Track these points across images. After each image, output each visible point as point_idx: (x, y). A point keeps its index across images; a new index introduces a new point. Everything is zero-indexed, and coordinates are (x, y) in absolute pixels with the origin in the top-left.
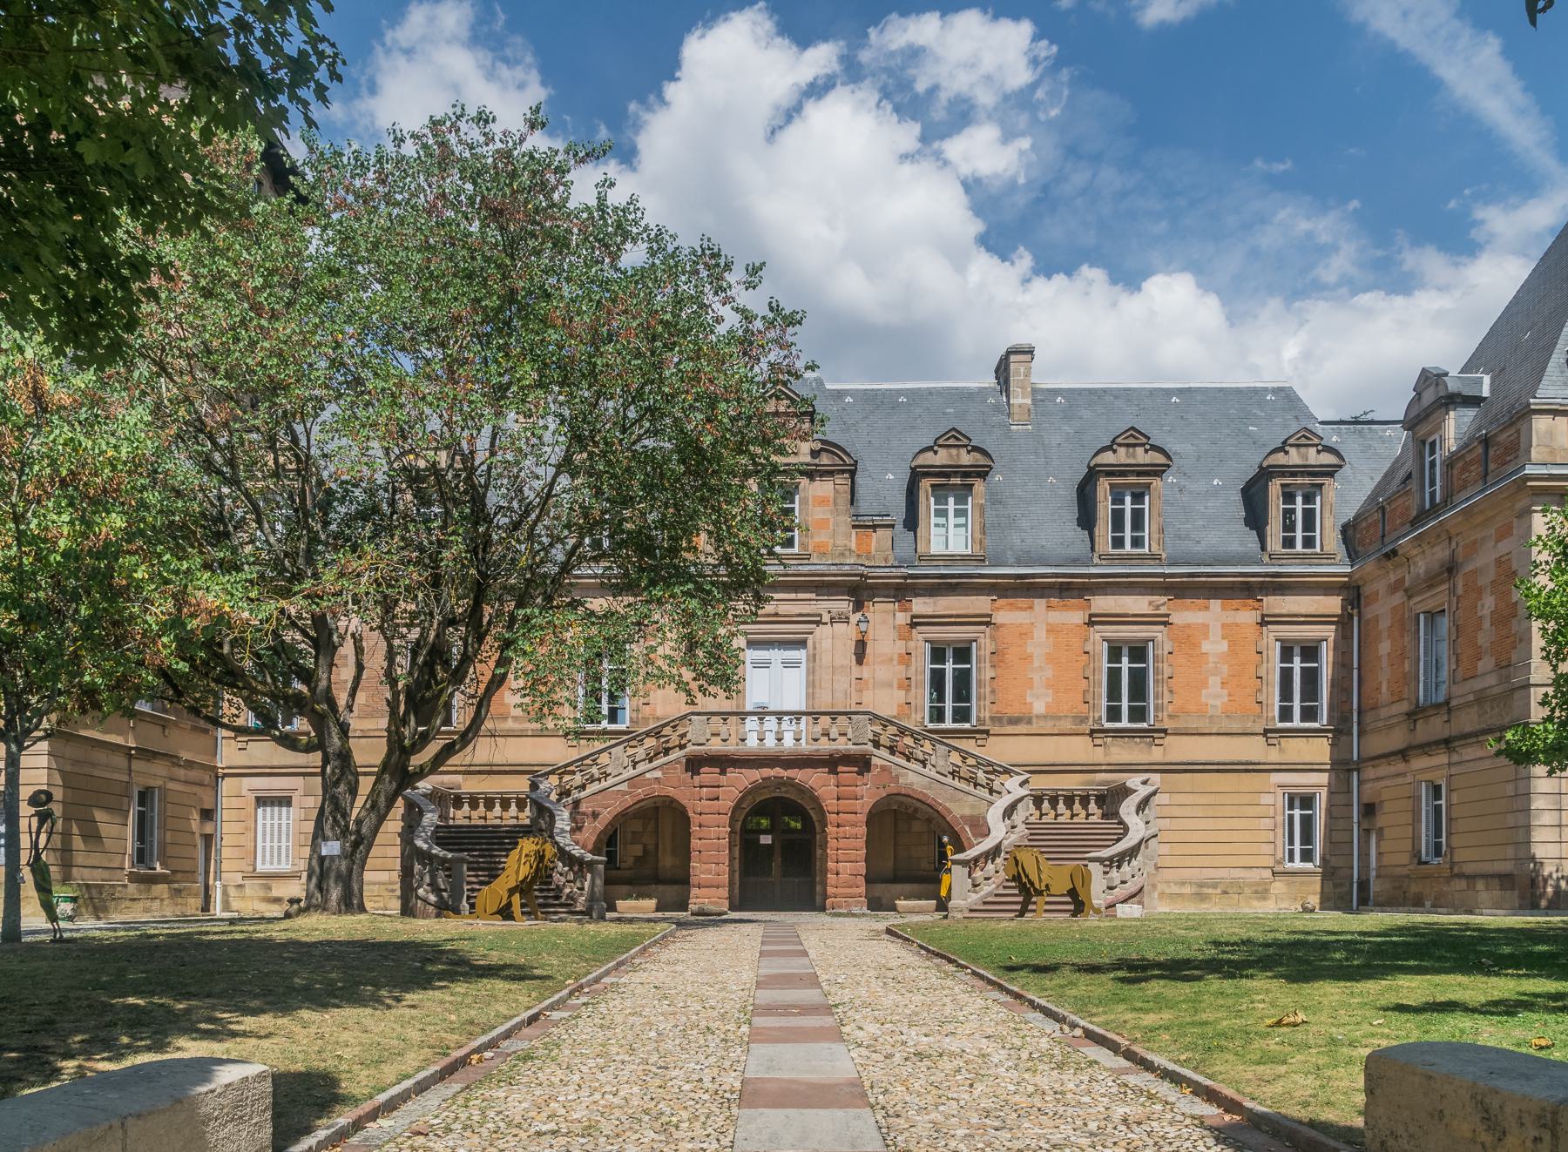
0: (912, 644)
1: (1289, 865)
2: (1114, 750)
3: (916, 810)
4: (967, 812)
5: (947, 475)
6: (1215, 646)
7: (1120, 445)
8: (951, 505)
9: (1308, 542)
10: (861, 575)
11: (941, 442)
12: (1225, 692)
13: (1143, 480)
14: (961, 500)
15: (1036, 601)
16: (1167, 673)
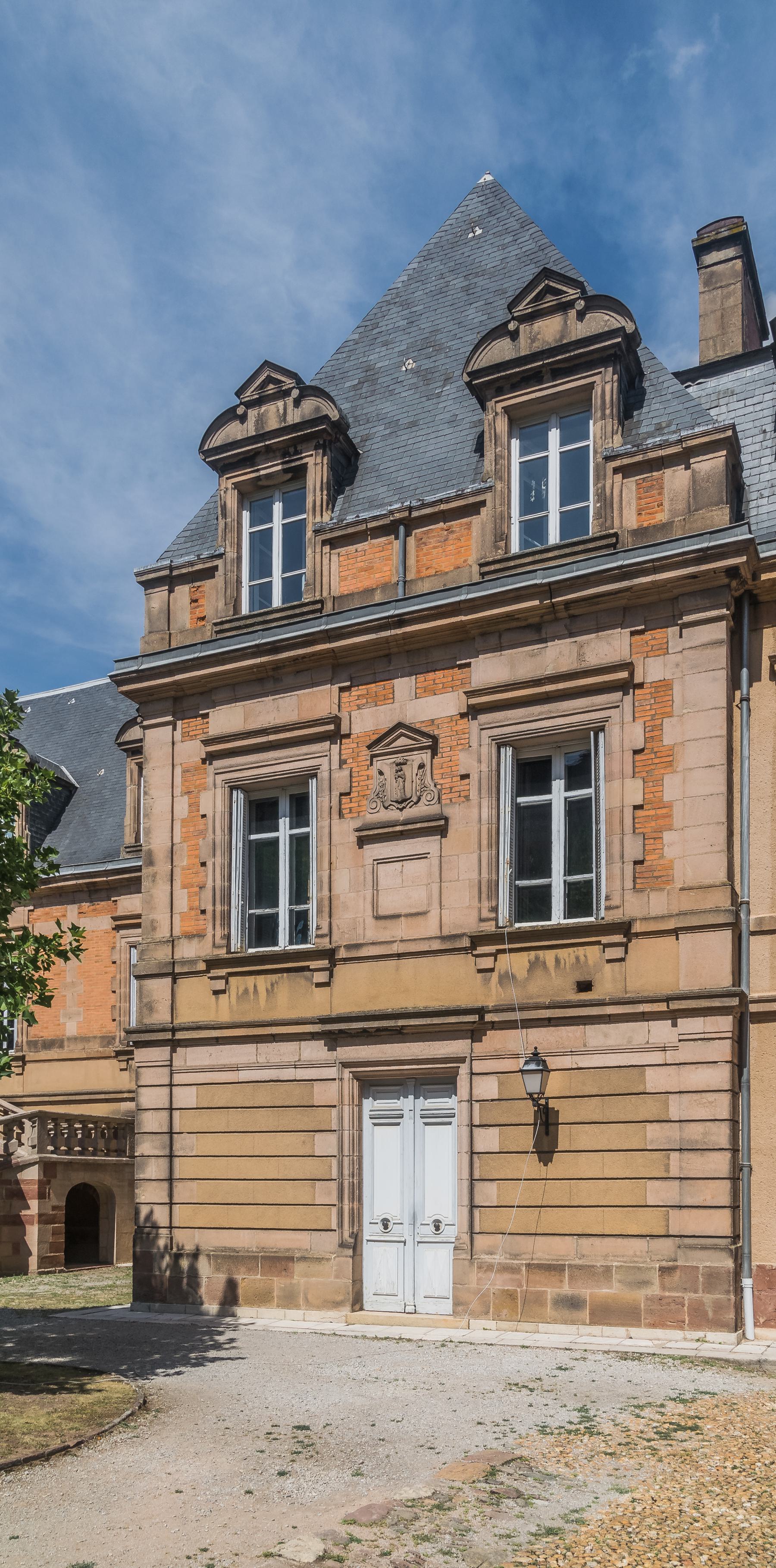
15: (70, 907)
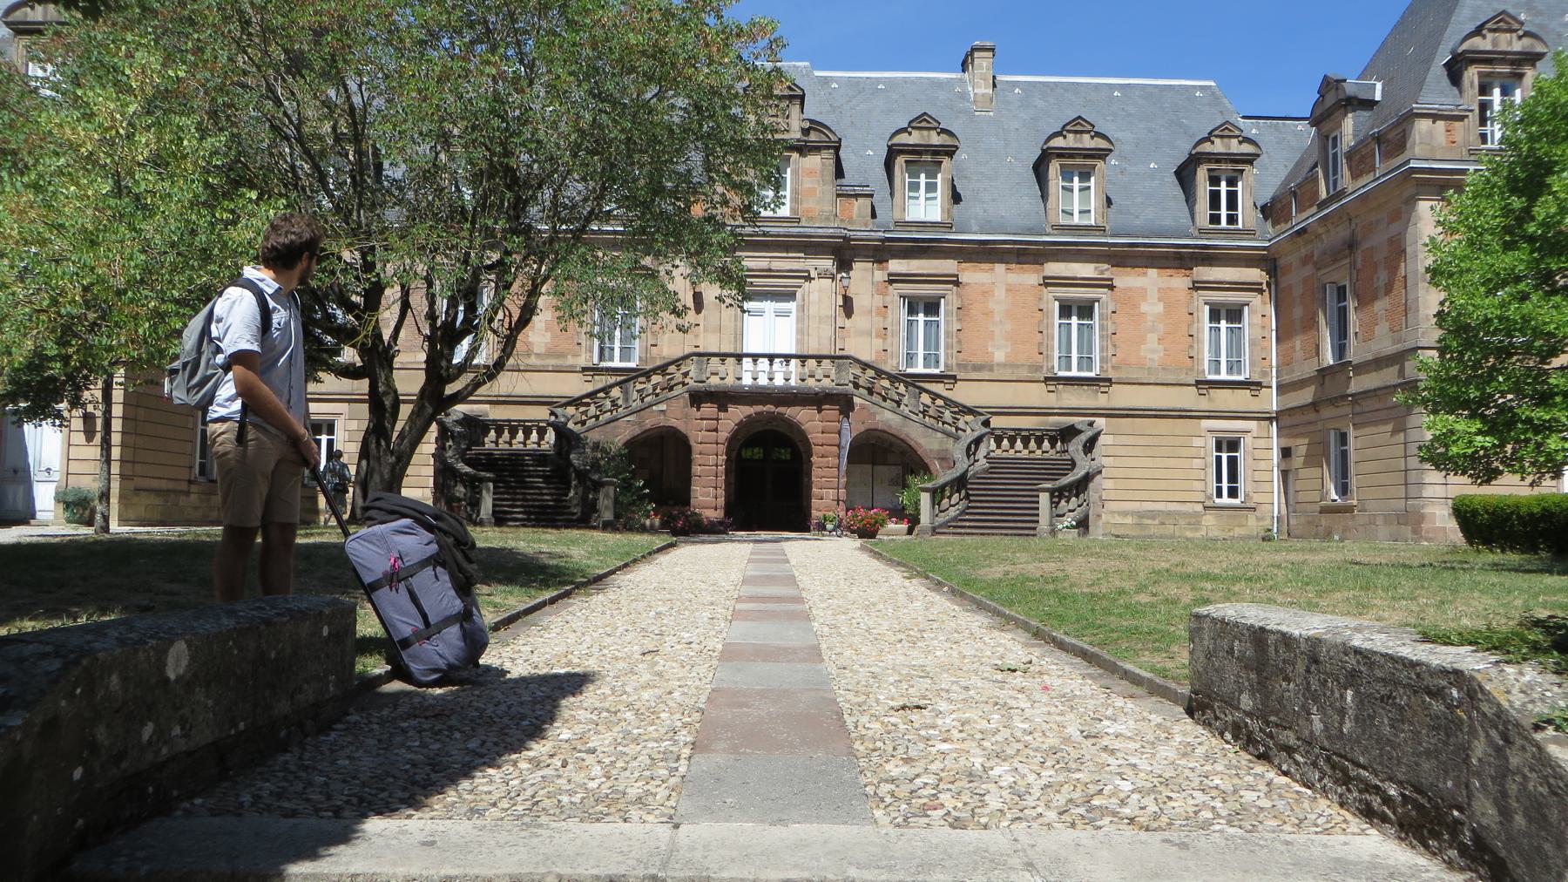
0: (888, 298)
1: (1218, 501)
2: (1065, 395)
3: (891, 444)
4: (936, 446)
5: (919, 153)
6: (1152, 308)
7: (1069, 131)
8: (923, 179)
9: (1232, 219)
10: (844, 238)
11: (914, 124)
12: (1161, 347)
13: (1089, 162)
14: (931, 175)
16: (1111, 329)
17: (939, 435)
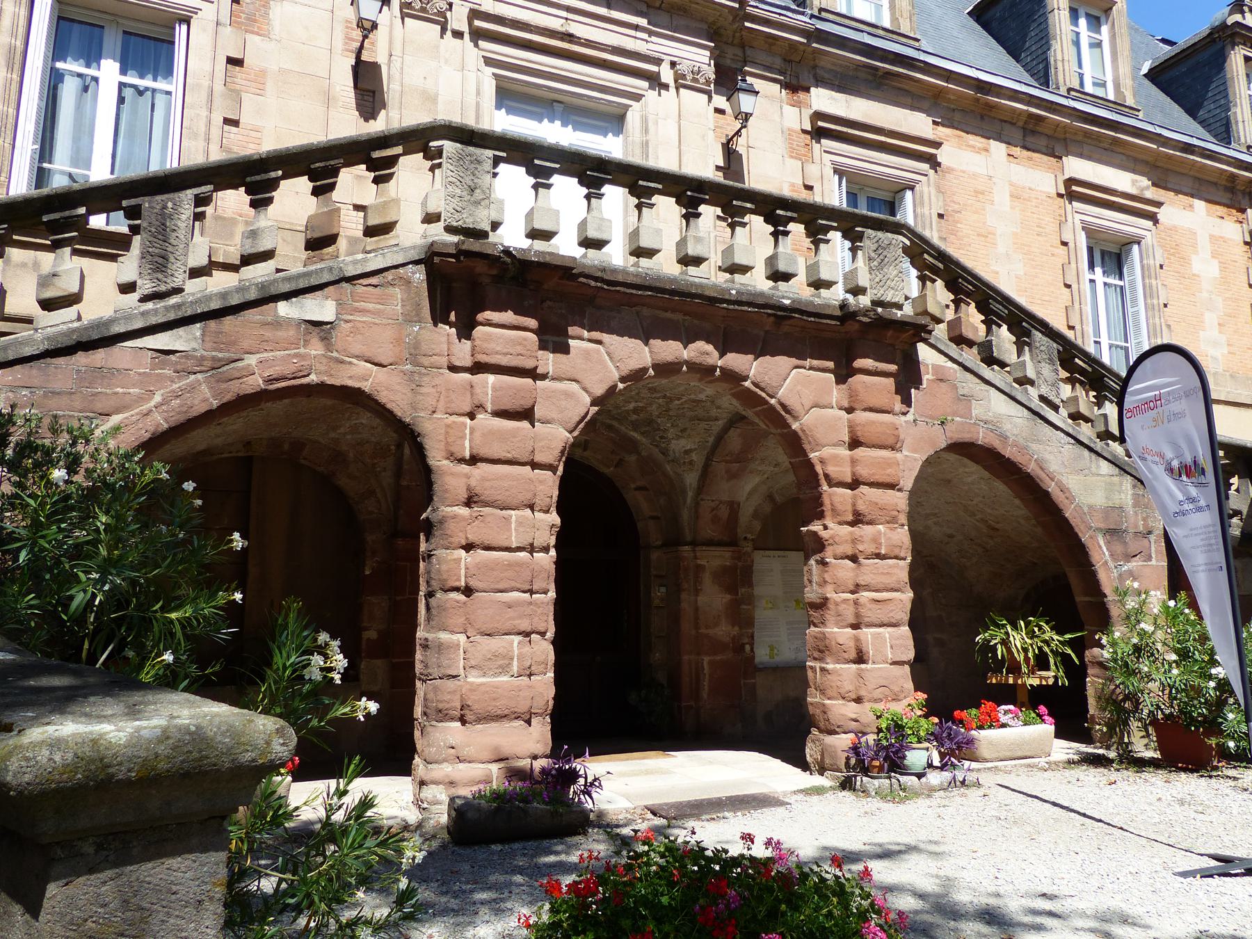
6: (1205, 266)
17: (1105, 467)
